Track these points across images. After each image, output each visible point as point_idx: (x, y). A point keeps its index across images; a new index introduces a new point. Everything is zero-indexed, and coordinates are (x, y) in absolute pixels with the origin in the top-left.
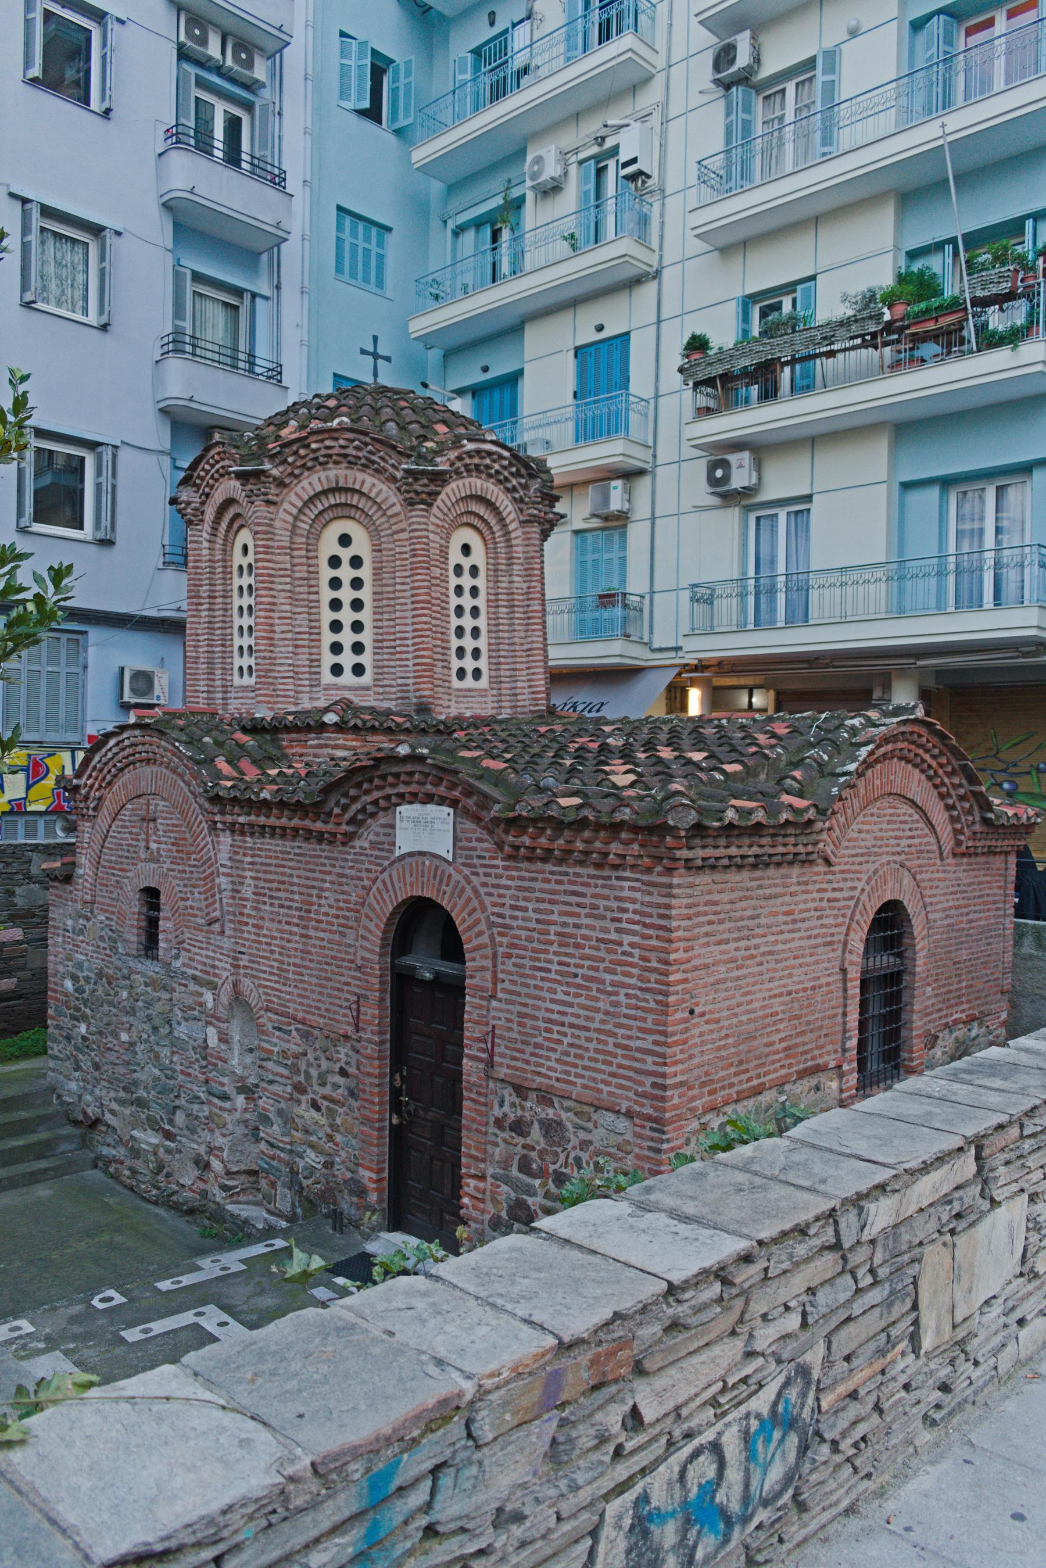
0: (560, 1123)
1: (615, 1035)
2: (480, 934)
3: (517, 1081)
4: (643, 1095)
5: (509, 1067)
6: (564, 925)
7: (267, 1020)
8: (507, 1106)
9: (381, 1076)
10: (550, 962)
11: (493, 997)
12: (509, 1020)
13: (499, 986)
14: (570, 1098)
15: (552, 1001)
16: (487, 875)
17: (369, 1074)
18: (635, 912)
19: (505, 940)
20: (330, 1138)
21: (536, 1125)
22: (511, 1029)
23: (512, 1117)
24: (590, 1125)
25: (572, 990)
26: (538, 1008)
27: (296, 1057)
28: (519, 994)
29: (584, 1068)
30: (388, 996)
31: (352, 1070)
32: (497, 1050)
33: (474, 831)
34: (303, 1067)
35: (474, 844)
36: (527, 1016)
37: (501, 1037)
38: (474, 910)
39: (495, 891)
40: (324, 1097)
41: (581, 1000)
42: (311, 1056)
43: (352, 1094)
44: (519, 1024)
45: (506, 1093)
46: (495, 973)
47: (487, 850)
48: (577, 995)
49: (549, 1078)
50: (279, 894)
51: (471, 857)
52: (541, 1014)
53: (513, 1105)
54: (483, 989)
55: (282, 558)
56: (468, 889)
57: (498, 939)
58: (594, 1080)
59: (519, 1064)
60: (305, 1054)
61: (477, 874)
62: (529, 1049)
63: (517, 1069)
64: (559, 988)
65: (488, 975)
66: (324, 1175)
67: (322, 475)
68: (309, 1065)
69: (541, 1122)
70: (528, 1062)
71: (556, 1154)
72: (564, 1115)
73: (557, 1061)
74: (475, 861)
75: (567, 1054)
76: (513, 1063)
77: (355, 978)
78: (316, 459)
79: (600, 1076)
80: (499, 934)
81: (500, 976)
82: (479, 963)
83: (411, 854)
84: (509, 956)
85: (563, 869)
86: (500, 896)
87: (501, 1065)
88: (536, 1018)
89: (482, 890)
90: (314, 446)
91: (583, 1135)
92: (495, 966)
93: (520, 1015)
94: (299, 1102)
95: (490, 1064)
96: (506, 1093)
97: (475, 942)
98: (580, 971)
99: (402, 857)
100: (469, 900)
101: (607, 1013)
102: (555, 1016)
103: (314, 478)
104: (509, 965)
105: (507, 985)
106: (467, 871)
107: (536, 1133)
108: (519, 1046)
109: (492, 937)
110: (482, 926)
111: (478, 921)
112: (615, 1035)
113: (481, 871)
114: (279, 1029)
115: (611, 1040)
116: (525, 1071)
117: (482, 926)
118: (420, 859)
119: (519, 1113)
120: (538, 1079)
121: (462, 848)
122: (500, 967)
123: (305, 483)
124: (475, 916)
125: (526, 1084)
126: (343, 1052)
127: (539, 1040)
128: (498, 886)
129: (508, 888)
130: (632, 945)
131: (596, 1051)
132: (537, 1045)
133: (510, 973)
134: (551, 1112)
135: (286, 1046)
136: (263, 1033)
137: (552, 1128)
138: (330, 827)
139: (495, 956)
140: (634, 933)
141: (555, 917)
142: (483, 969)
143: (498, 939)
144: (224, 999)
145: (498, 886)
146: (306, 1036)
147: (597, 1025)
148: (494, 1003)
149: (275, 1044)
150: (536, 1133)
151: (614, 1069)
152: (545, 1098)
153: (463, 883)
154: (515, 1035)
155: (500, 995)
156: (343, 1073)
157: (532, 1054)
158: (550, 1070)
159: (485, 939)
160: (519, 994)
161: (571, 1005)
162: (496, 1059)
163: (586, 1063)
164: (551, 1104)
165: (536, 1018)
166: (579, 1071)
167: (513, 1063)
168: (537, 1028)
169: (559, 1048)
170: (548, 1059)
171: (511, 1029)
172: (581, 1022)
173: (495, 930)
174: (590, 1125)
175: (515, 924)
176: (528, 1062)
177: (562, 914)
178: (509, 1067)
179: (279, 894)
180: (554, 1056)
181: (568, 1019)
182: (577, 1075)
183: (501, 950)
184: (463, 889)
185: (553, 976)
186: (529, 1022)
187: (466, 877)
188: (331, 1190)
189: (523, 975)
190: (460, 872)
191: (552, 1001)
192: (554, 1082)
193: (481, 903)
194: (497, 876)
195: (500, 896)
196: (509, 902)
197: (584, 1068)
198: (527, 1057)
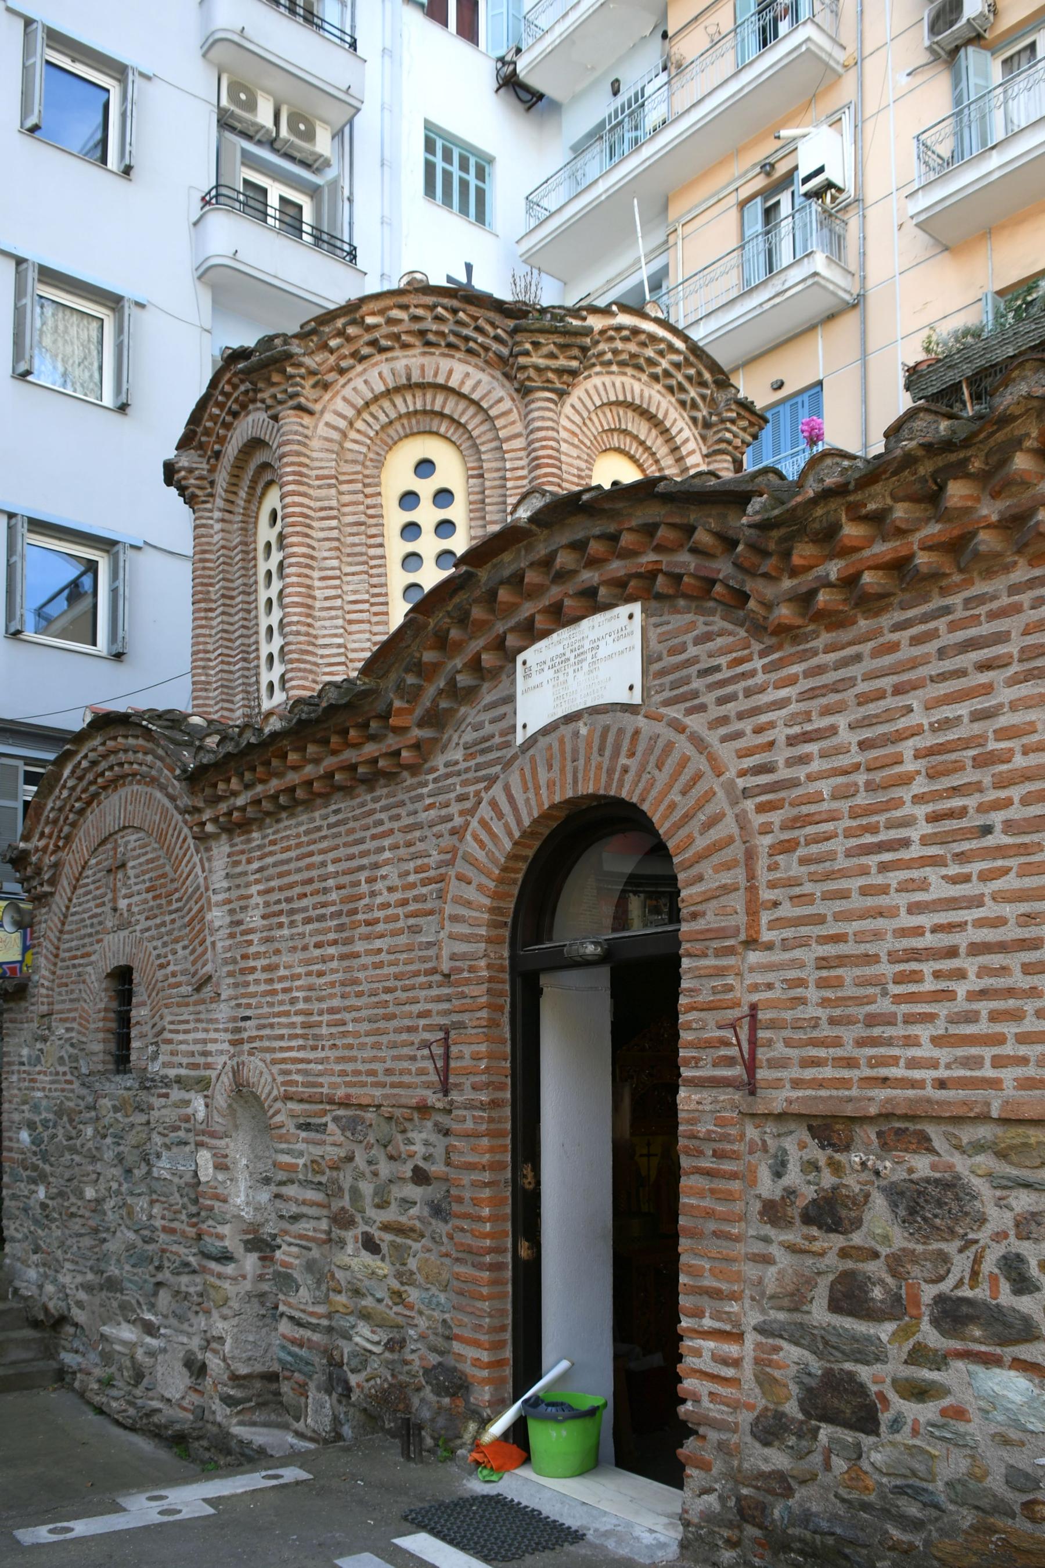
2: (714, 821)
3: (821, 1109)
5: (796, 1084)
7: (284, 1116)
8: (800, 1169)
9: (495, 1167)
11: (751, 943)
12: (801, 983)
13: (765, 917)
14: (984, 1118)
16: (721, 701)
17: (470, 1167)
19: (776, 817)
20: (398, 1297)
21: (879, 1202)
22: (802, 1001)
27: (335, 1168)
28: (820, 920)
30: (506, 1019)
31: (436, 1168)
32: (762, 1054)
33: (691, 626)
34: (346, 1182)
35: (692, 651)
36: (842, 960)
37: (773, 1025)
38: (698, 777)
39: (747, 726)
40: (386, 1227)
42: (360, 1160)
43: (438, 1211)
44: (823, 984)
45: (789, 1144)
46: (752, 890)
47: (722, 652)
49: (914, 1084)
51: (687, 680)
52: (881, 949)
53: (811, 1166)
55: (323, 492)
57: (758, 820)
59: (828, 1072)
60: (350, 1159)
61: (702, 708)
62: (849, 1034)
63: (821, 1084)
66: (388, 1363)
67: (385, 368)
68: (360, 1175)
69: (894, 1193)
70: (850, 1063)
71: (944, 1258)
73: (937, 1041)
74: (697, 684)
76: (809, 1073)
78: (374, 343)
80: (761, 808)
81: (767, 895)
82: (713, 880)
84: (787, 847)
86: (758, 730)
87: (776, 1084)
88: (871, 959)
89: (712, 738)
90: (370, 320)
92: (751, 876)
93: (823, 963)
94: (342, 1243)
95: (751, 1087)
96: (789, 1144)
100: (684, 761)
103: (373, 375)
104: (791, 866)
105: (787, 910)
107: (880, 1223)
108: (826, 1031)
109: (742, 821)
110: (721, 802)
111: (710, 795)
113: (709, 699)
114: (306, 1127)
116: (845, 1083)
117: (721, 802)
120: (882, 1094)
121: (662, 673)
122: (763, 876)
123: (359, 383)
124: (701, 787)
125: (849, 1110)
126: (421, 1141)
129: (780, 704)
132: (871, 1021)
133: (792, 882)
134: (922, 1165)
135: (317, 1151)
136: (282, 1138)
139: (750, 856)
142: (727, 890)
143: (758, 820)
144: (221, 1101)
146: (350, 1126)
148: (754, 957)
149: (301, 1150)
150: (880, 1223)
152: (902, 1129)
154: (812, 1011)
155: (766, 936)
156: (420, 1177)
157: (861, 1043)
158: (921, 1062)
159: (728, 827)
160: (820, 920)
162: (761, 1074)
164: (924, 1144)
167: (809, 1073)
171: (802, 1001)
173: (750, 805)
176: (850, 1063)
178: (796, 1084)
180: (923, 1032)
183: (767, 840)
184: (669, 746)
186: (848, 974)
188: (402, 1386)
189: (828, 876)
192: (930, 1092)
193: (712, 759)
194: (749, 693)
195: (758, 730)
196: (780, 734)
198: (848, 1050)
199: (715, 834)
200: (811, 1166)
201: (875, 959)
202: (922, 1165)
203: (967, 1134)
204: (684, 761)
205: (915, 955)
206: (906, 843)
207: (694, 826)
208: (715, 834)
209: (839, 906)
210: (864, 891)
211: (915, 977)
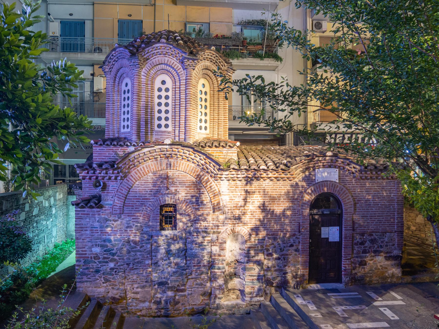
0: (375, 239)
1: (390, 216)
4: (399, 227)
6: (375, 194)
10: (371, 203)
15: (372, 212)
18: (394, 189)
23: (360, 241)
24: (384, 237)
25: (377, 208)
26: (368, 214)
29: (382, 225)
38: (347, 193)
41: (381, 210)
48: (379, 209)
50: (257, 198)
54: (350, 212)
56: (344, 189)
58: (385, 227)
59: (362, 228)
64: (373, 208)
65: (353, 209)
72: (376, 237)
75: (377, 223)
76: (360, 228)
77: (298, 218)
79: (386, 226)
83: (321, 182)
85: (374, 181)
91: (382, 240)
97: (347, 201)
98: (379, 204)
99: (319, 182)
100: (345, 191)
101: (388, 211)
102: (373, 215)
106: (343, 184)
110: (350, 197)
111: (348, 196)
112: (390, 216)
115: (389, 217)
118: (326, 183)
119: (362, 240)
127: (369, 221)
128: (354, 187)
130: (394, 196)
131: (385, 220)
132: (367, 223)
137: (373, 241)
138: (289, 176)
140: (395, 193)
141: (372, 192)
145: (354, 187)
147: (385, 215)
151: (390, 223)
153: (343, 187)
161: (378, 212)
163: (383, 224)
165: (367, 216)
166: (381, 226)
167: (360, 228)
168: (368, 219)
169: (374, 222)
170: (371, 225)
172: (381, 215)
174: (384, 237)
175: (359, 195)
177: (374, 191)
179: (257, 198)
181: (376, 215)
182: (380, 227)
184: (342, 189)
185: (372, 206)
187: (343, 186)
190: (341, 185)
191: (372, 212)
195: (354, 189)
197: (382, 225)
199: (349, 201)
200: (360, 238)
201: (367, 216)
202: (372, 237)
203: (377, 234)
204: (345, 191)
205: (372, 216)
206: (371, 205)
207: (346, 199)
208: (349, 201)
209: (364, 210)
210: (367, 209)
211: (372, 219)
